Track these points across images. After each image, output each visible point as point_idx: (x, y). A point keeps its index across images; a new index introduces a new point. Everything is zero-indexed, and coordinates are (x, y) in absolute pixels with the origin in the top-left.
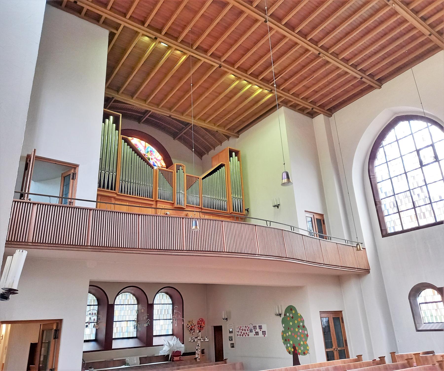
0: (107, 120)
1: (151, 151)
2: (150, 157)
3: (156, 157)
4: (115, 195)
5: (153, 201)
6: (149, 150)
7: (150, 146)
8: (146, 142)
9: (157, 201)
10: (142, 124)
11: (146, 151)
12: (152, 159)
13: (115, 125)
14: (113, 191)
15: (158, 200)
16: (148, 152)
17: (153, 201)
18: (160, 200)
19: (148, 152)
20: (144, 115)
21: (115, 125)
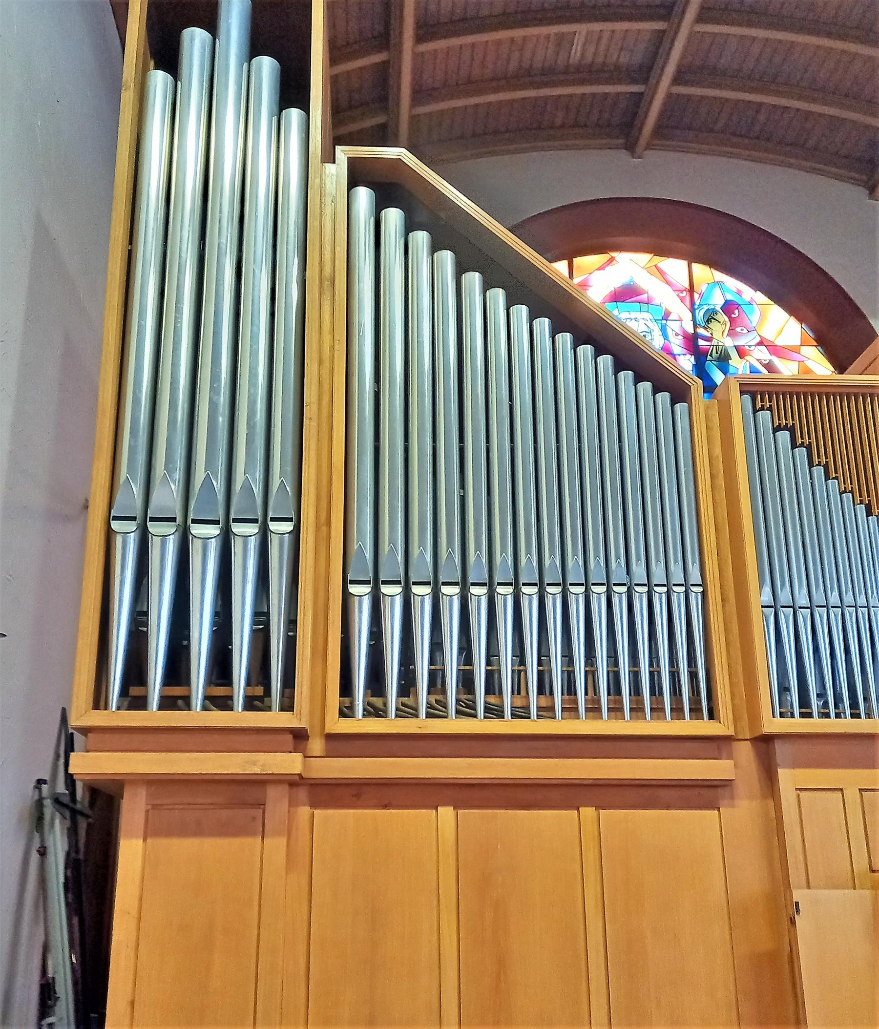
0: (195, 39)
1: (729, 307)
2: (729, 343)
3: (769, 333)
4: (289, 763)
5: (715, 745)
6: (717, 301)
7: (719, 276)
8: (692, 258)
9: (765, 743)
10: (654, 157)
11: (700, 315)
12: (741, 352)
13: (267, 65)
14: (239, 717)
15: (773, 725)
16: (710, 317)
17: (715, 745)
18: (797, 724)
19: (710, 317)
20: (646, 81)
21: (267, 65)
